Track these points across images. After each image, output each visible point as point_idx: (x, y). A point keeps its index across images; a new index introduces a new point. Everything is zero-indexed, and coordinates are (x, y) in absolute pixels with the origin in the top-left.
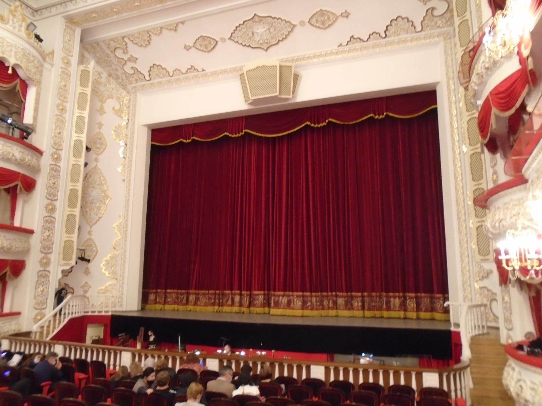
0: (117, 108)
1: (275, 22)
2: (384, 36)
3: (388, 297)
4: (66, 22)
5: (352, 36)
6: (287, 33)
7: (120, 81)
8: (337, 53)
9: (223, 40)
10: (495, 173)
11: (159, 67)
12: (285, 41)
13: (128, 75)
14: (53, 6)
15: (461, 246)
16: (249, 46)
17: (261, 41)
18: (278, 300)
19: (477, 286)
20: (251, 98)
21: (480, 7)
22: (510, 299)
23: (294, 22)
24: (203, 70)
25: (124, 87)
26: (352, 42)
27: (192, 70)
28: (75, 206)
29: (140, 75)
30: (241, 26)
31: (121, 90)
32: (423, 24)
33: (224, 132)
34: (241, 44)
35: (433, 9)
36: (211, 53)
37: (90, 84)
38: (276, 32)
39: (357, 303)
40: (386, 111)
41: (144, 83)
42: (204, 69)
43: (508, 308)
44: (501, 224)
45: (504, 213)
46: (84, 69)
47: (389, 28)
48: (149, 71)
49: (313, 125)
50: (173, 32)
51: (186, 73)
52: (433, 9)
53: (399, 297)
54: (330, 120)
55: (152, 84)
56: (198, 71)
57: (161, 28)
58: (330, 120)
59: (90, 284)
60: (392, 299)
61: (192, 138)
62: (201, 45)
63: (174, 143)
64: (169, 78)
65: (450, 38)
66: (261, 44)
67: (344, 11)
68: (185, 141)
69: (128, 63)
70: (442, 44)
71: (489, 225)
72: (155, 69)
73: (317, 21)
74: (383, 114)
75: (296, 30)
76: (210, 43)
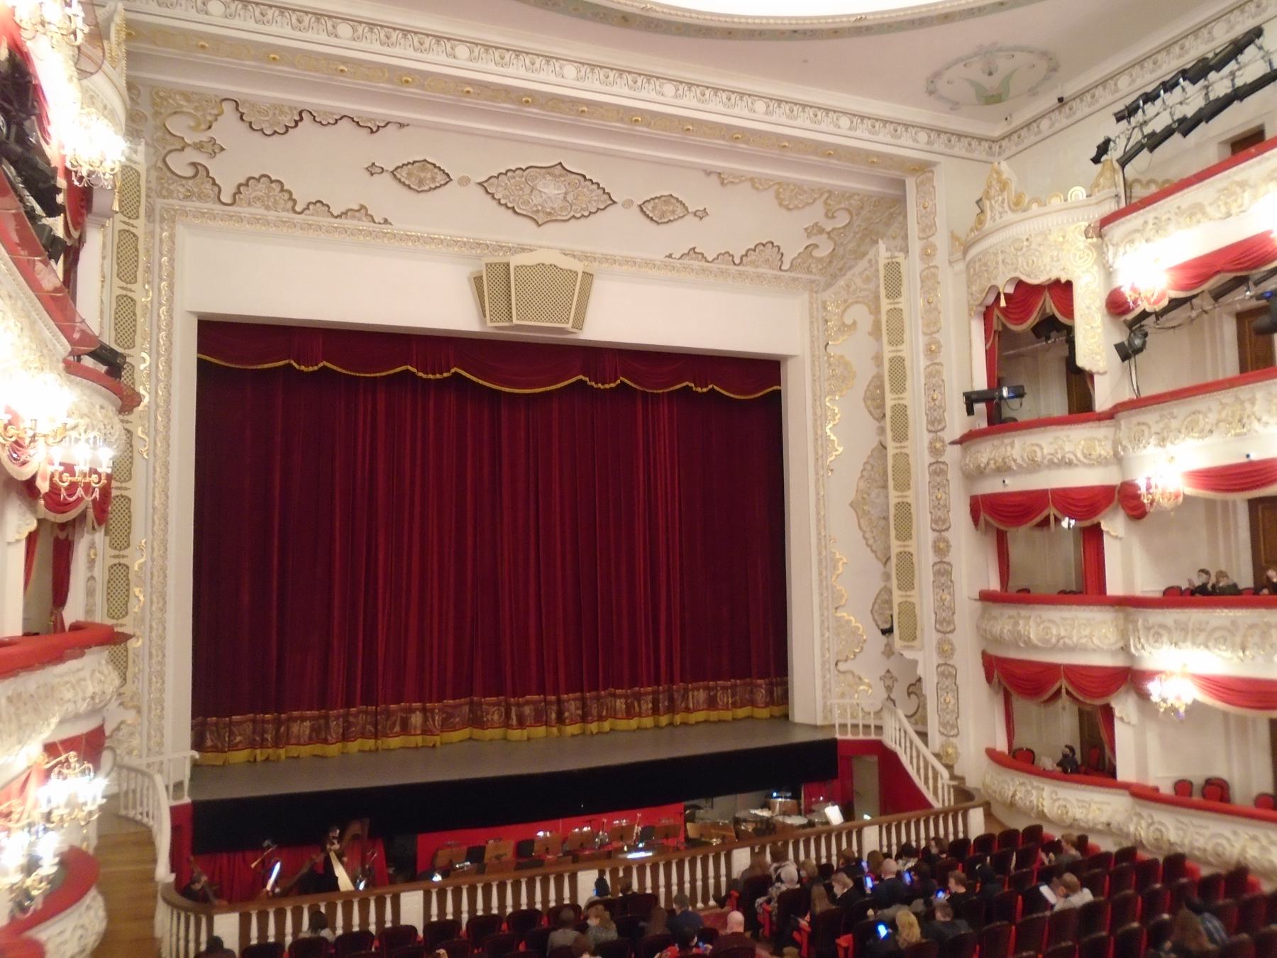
2: (737, 261)
9: (464, 181)
13: (169, 174)
20: (515, 321)
24: (386, 221)
29: (209, 186)
35: (816, 246)
39: (647, 705)
41: (210, 205)
48: (240, 185)
52: (816, 246)
53: (707, 688)
61: (321, 365)
62: (410, 174)
63: (266, 366)
66: (538, 211)
68: (303, 368)
69: (187, 150)
70: (806, 296)
71: (1032, 636)
76: (433, 179)
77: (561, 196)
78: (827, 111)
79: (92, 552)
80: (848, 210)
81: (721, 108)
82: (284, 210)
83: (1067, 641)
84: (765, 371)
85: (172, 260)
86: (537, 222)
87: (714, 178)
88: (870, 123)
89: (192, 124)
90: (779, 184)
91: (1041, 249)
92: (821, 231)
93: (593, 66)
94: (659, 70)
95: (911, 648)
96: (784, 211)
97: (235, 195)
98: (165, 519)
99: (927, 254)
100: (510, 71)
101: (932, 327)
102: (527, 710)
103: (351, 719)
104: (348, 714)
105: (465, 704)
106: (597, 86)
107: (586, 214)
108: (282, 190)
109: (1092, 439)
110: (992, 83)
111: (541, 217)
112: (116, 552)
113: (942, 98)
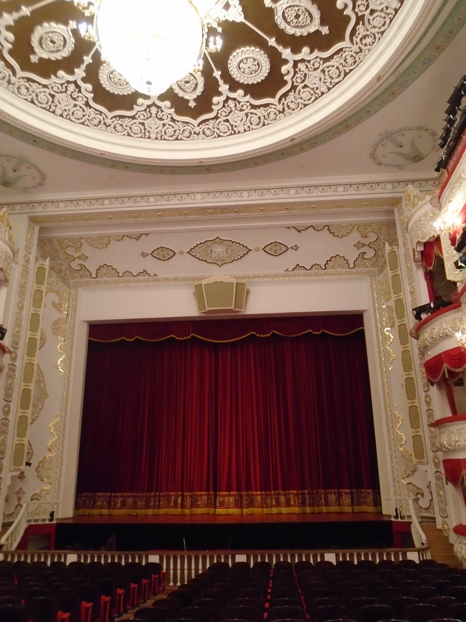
0: (57, 302)
2: (324, 268)
3: (326, 494)
4: (29, 221)
5: (298, 265)
7: (61, 275)
8: (283, 276)
9: (181, 253)
10: (427, 396)
11: (109, 268)
12: (239, 260)
13: (72, 270)
14: (18, 204)
15: (391, 449)
16: (206, 260)
18: (224, 500)
19: (405, 482)
20: (207, 309)
21: (411, 270)
22: (445, 493)
24: (155, 275)
25: (64, 280)
26: (297, 269)
27: (143, 274)
28: (28, 408)
29: (87, 272)
30: (201, 244)
31: (61, 284)
32: (356, 263)
33: (171, 334)
34: (198, 258)
37: (46, 282)
40: (323, 329)
43: (443, 501)
44: (456, 444)
45: (458, 437)
46: (41, 266)
47: (328, 262)
48: (97, 270)
49: (258, 335)
50: (134, 240)
51: (137, 276)
52: (364, 253)
54: (274, 331)
55: (97, 282)
56: (150, 276)
57: (124, 236)
58: (274, 331)
59: (24, 490)
60: (329, 496)
61: (135, 338)
62: (158, 254)
63: (114, 340)
64: (118, 278)
65: (374, 276)
66: (217, 260)
68: (128, 340)
70: (368, 279)
71: (445, 443)
72: (105, 269)
73: (270, 249)
75: (250, 253)
76: (168, 254)
77: (225, 252)
78: (330, 186)
79: (6, 409)
80: (372, 231)
81: (271, 197)
82: (115, 277)
83: (459, 443)
84: (354, 320)
85: (76, 302)
86: (219, 265)
88: (355, 186)
89: (74, 249)
91: (425, 223)
92: (364, 245)
93: (208, 193)
94: (239, 187)
95: (421, 463)
97: (96, 274)
98: (67, 404)
99: (405, 244)
100: (173, 202)
101: (411, 279)
106: (211, 200)
107: (239, 257)
108: (113, 269)
109: (454, 320)
110: (407, 150)
111: (220, 263)
112: (23, 411)
113: (387, 165)
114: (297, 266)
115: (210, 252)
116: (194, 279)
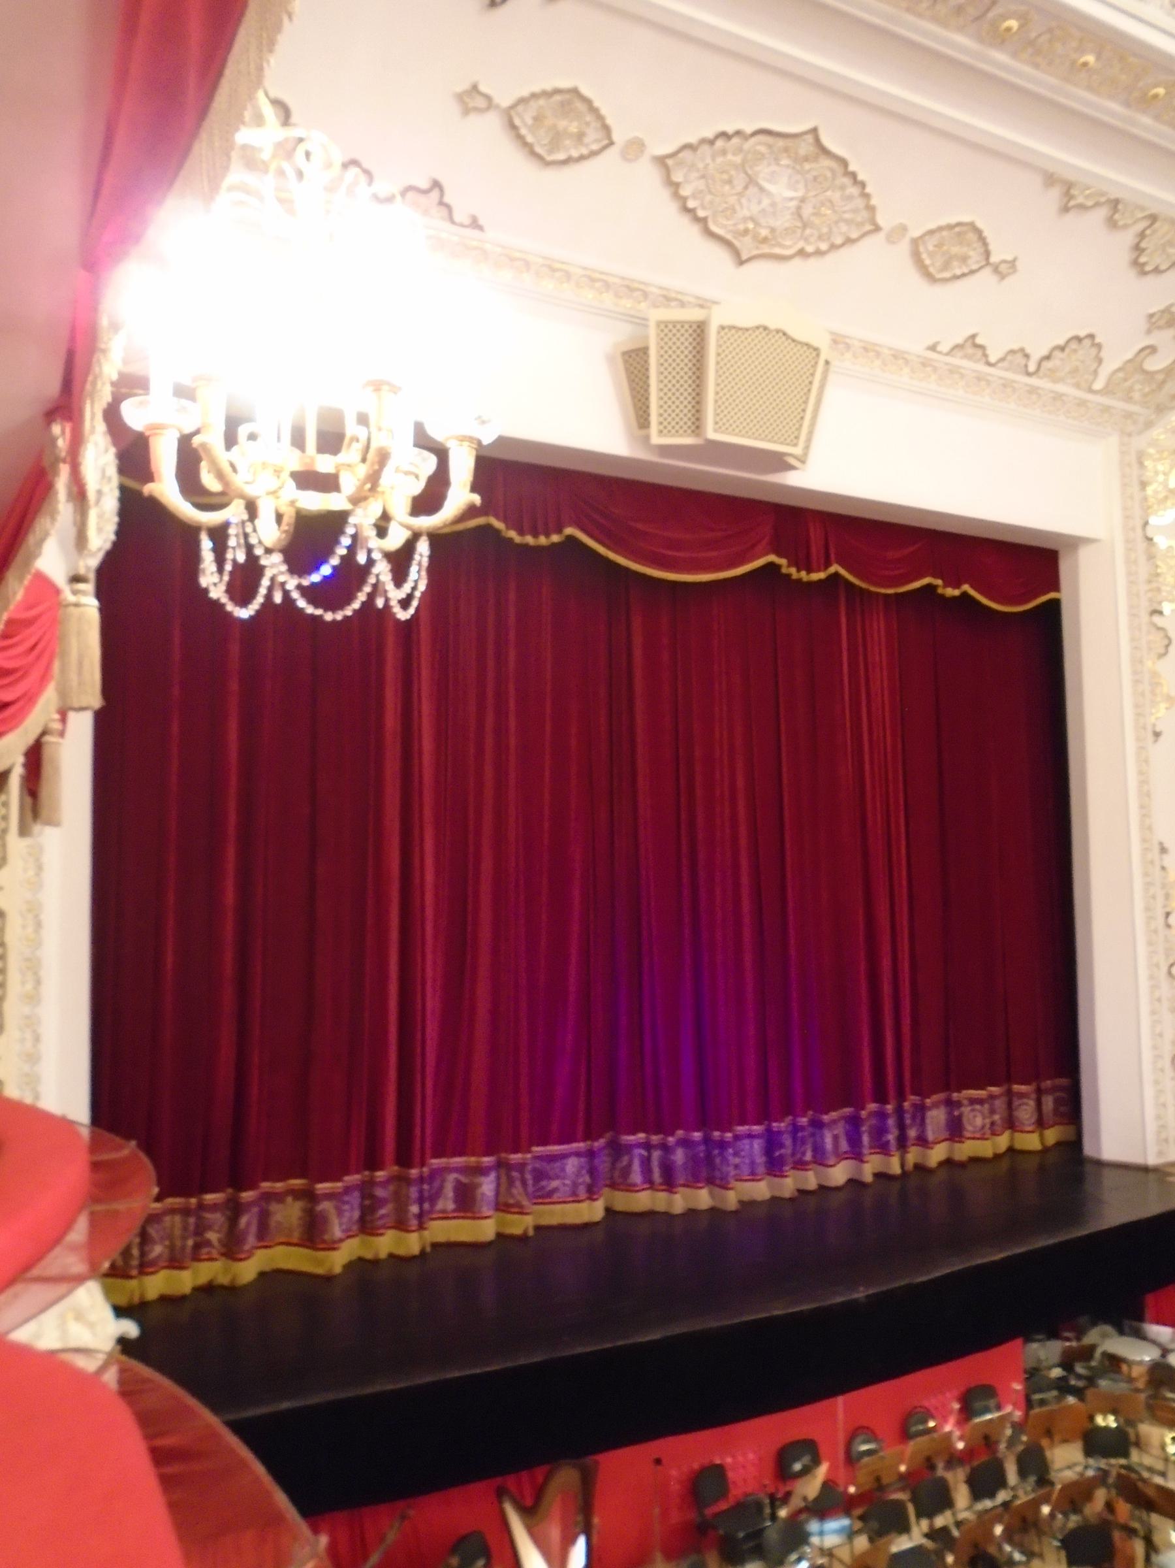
1: (843, 188)
2: (1032, 368)
5: (973, 336)
6: (839, 241)
16: (703, 221)
17: (751, 226)
20: (712, 434)
23: (880, 220)
24: (475, 224)
26: (960, 353)
27: (422, 199)
35: (1152, 349)
36: (551, 174)
38: (813, 218)
42: (481, 222)
62: (537, 119)
65: (1130, 435)
66: (746, 232)
67: (1010, 258)
70: (1114, 440)
74: (957, 586)
76: (580, 136)
77: (793, 204)
87: (1055, 193)
90: (1153, 218)
96: (1132, 274)
102: (679, 1156)
103: (380, 1192)
104: (372, 1183)
105: (578, 1154)
107: (824, 246)
114: (969, 343)
115: (739, 188)
116: (630, 288)
